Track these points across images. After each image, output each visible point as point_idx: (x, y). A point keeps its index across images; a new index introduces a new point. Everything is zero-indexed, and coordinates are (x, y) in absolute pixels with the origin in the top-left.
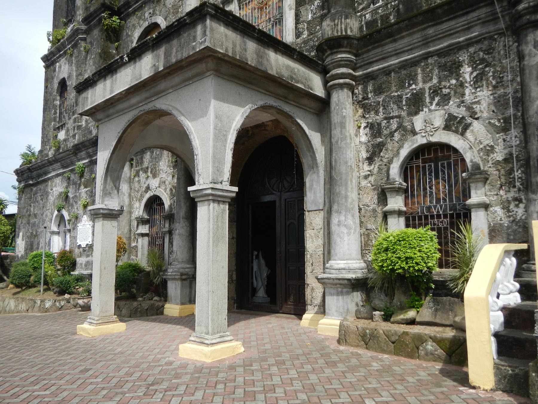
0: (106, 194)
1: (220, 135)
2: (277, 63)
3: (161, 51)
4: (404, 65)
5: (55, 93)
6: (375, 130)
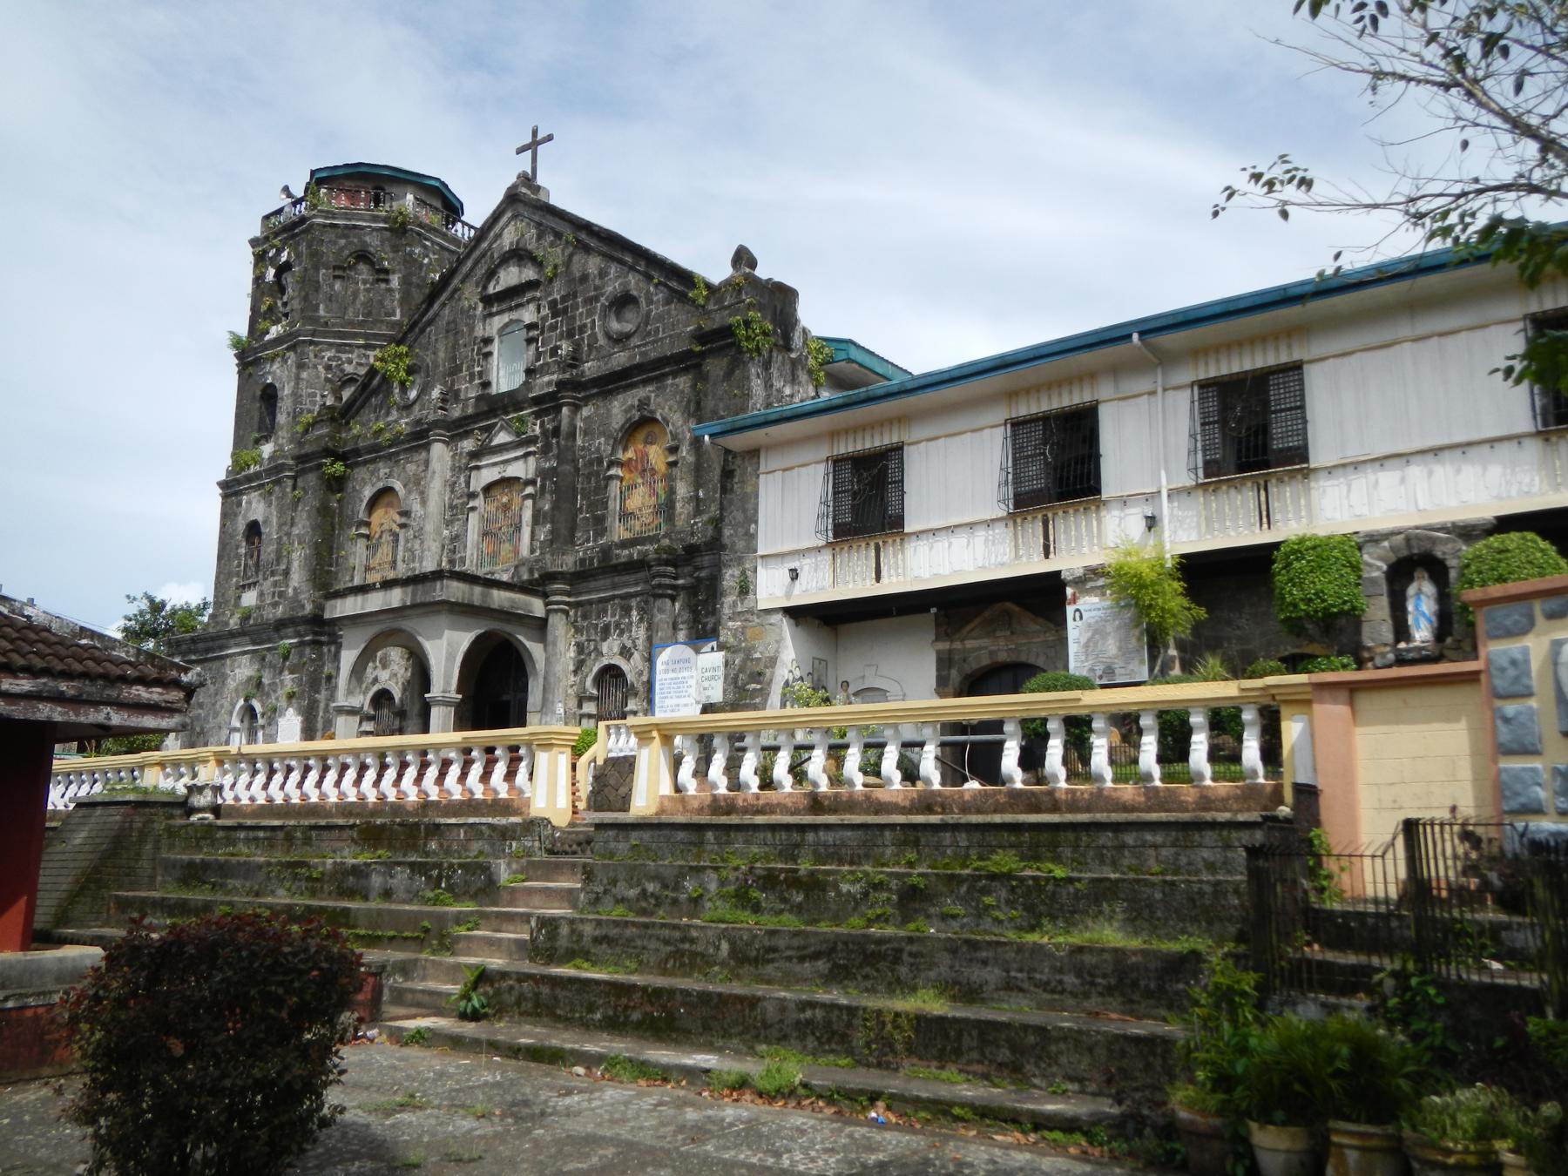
0: (350, 692)
1: (450, 657)
2: (499, 598)
3: (410, 589)
4: (601, 600)
5: (240, 537)
6: (580, 648)
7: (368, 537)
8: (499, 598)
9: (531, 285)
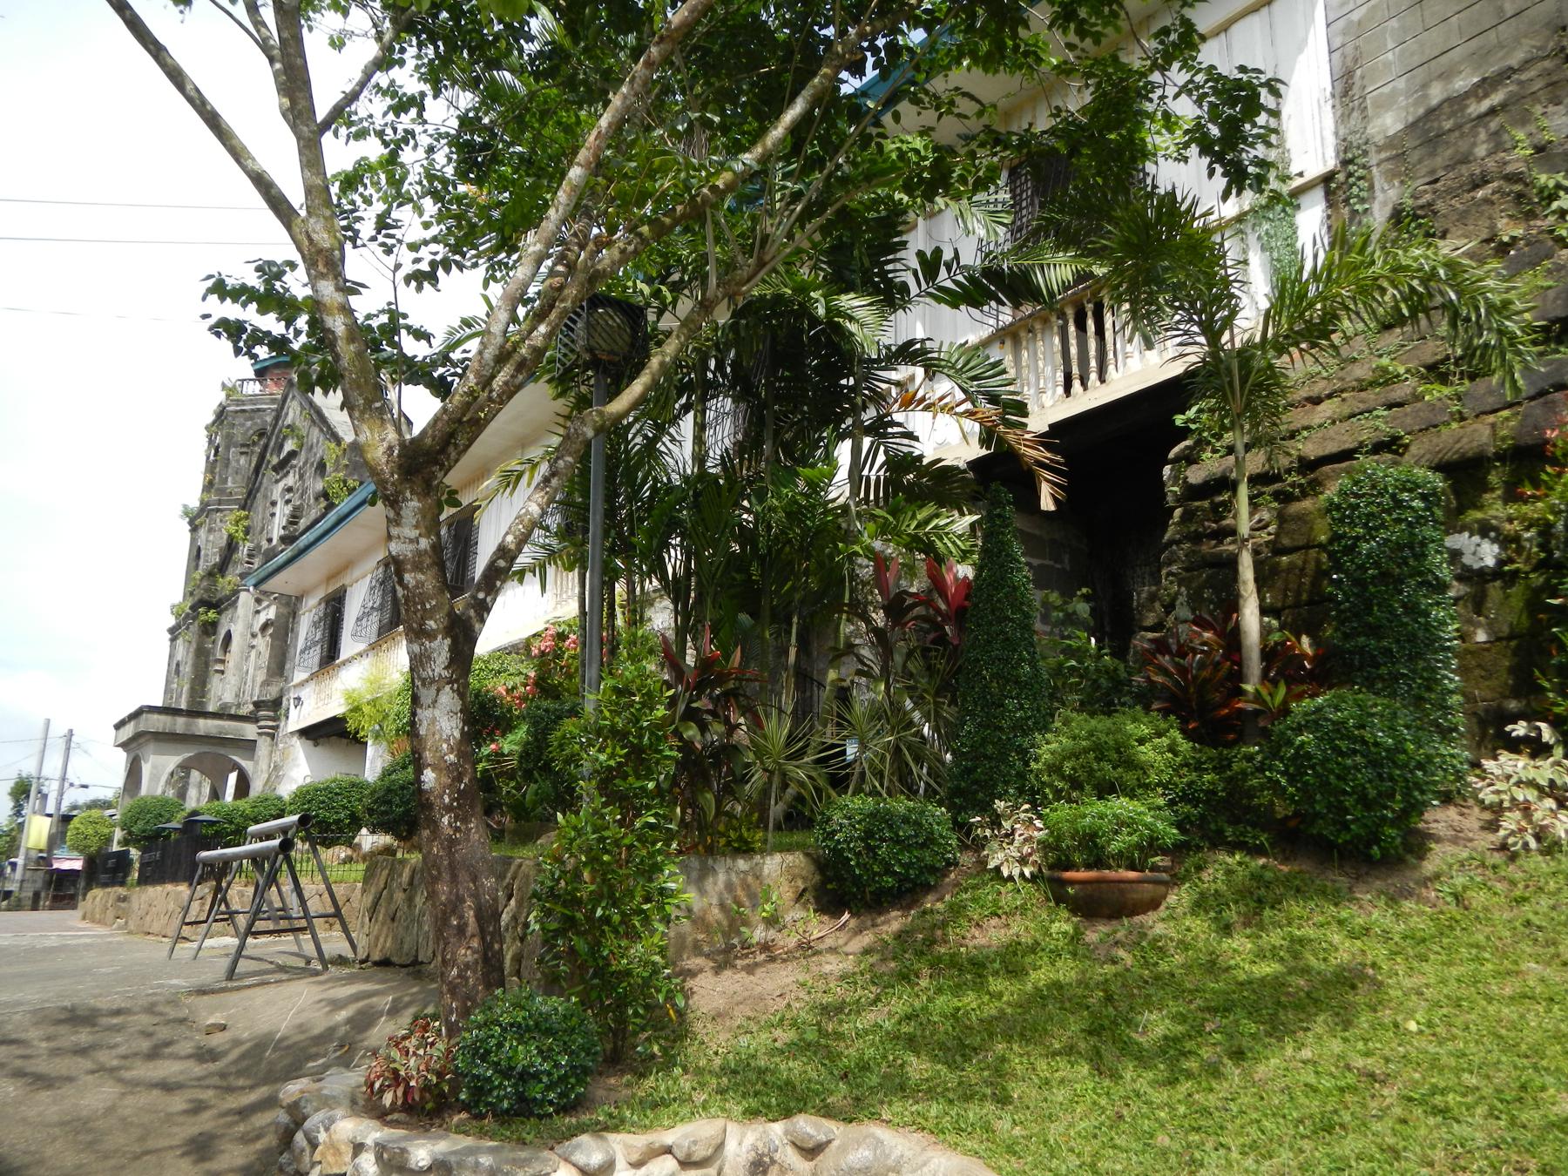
7: (222, 672)
8: (204, 726)
9: (293, 454)
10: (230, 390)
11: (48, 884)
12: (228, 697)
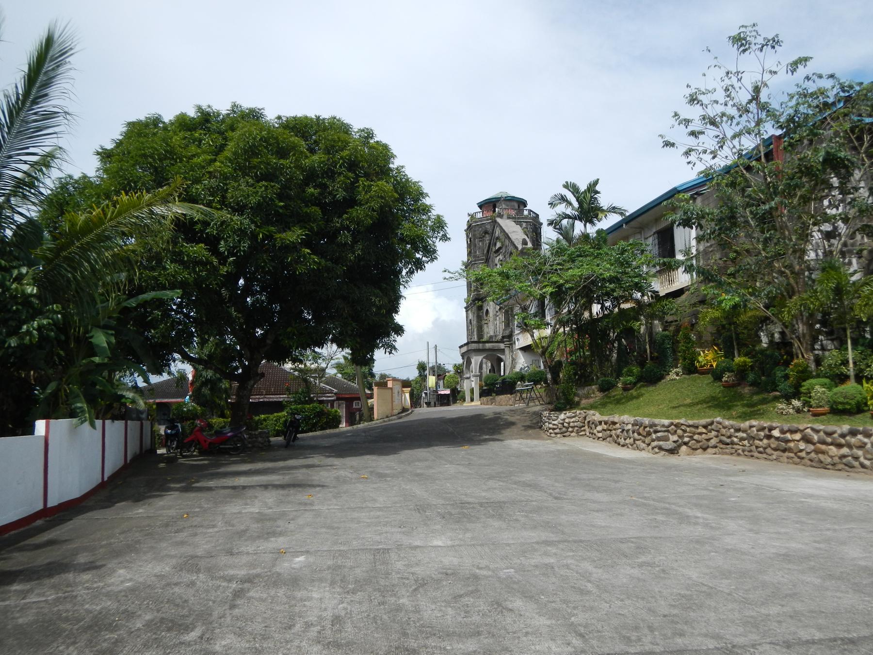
8: (488, 346)
9: (500, 248)
10: (472, 216)
11: (438, 400)
12: (492, 333)
